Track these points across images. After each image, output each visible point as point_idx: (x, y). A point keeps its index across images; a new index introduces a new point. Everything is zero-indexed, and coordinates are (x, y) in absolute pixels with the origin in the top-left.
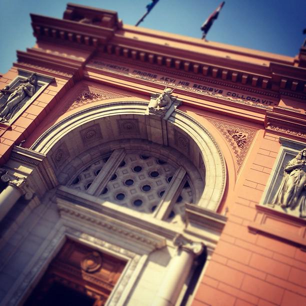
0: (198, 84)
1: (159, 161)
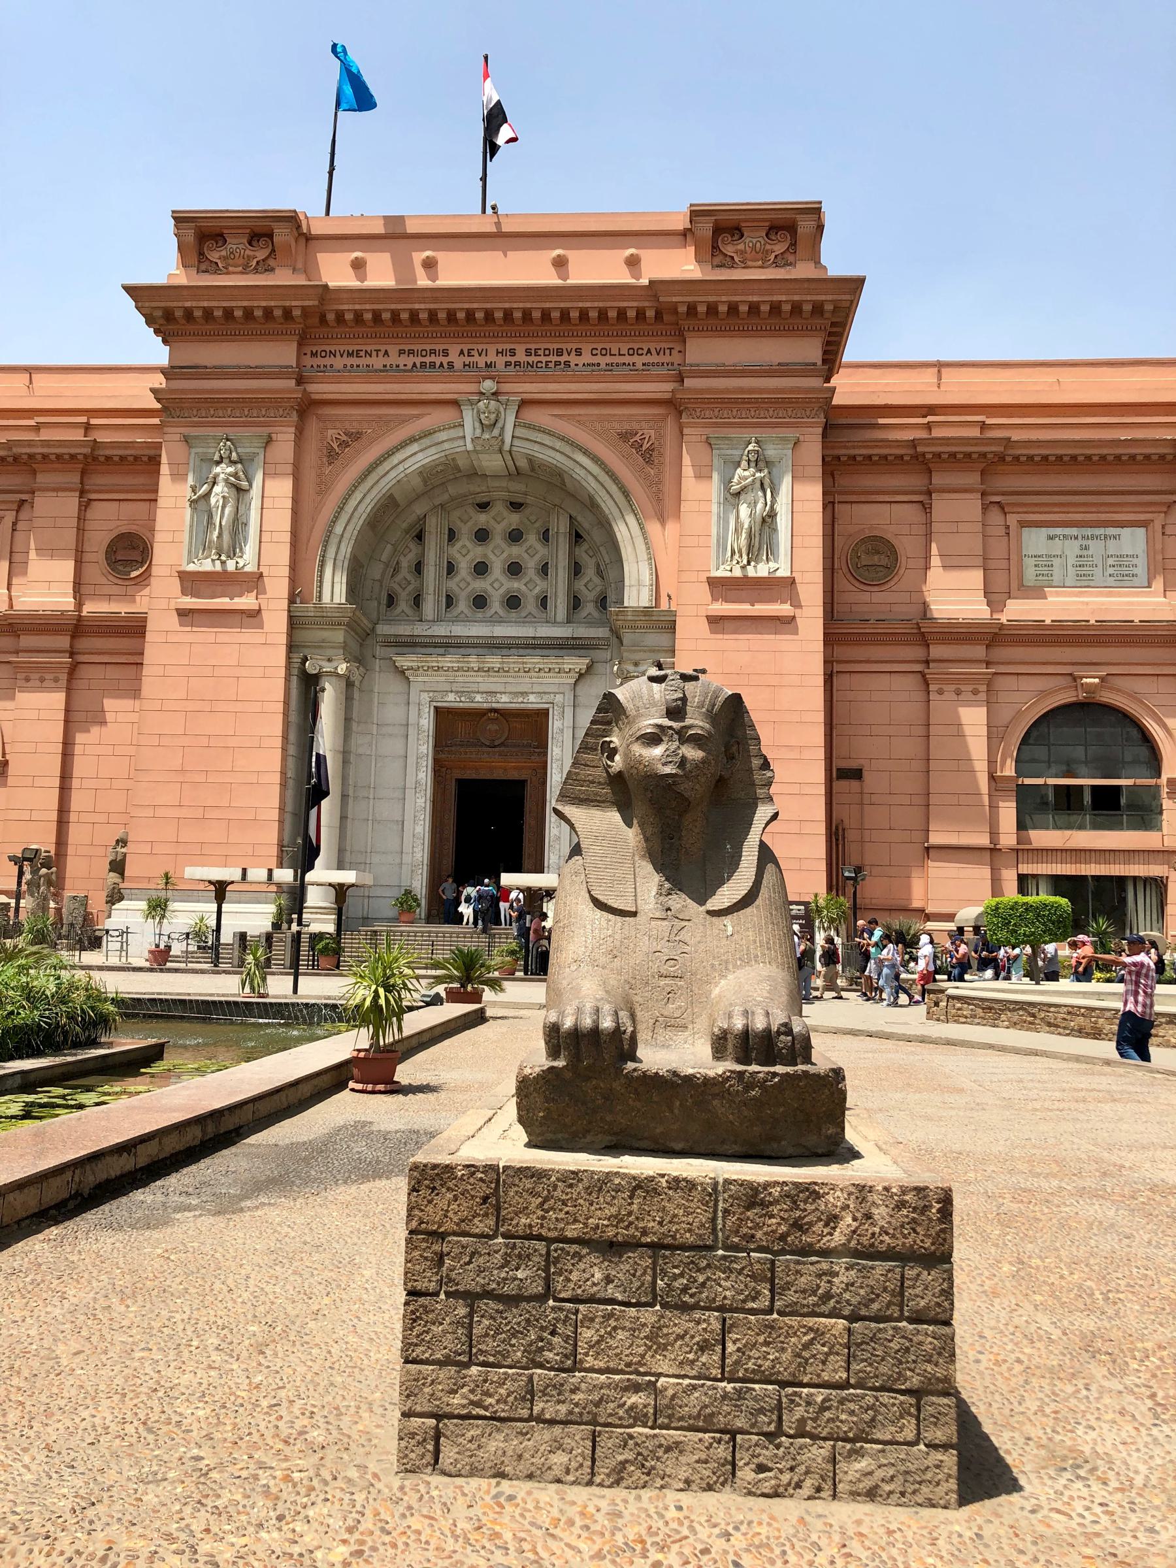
0: (533, 346)
1: (511, 503)
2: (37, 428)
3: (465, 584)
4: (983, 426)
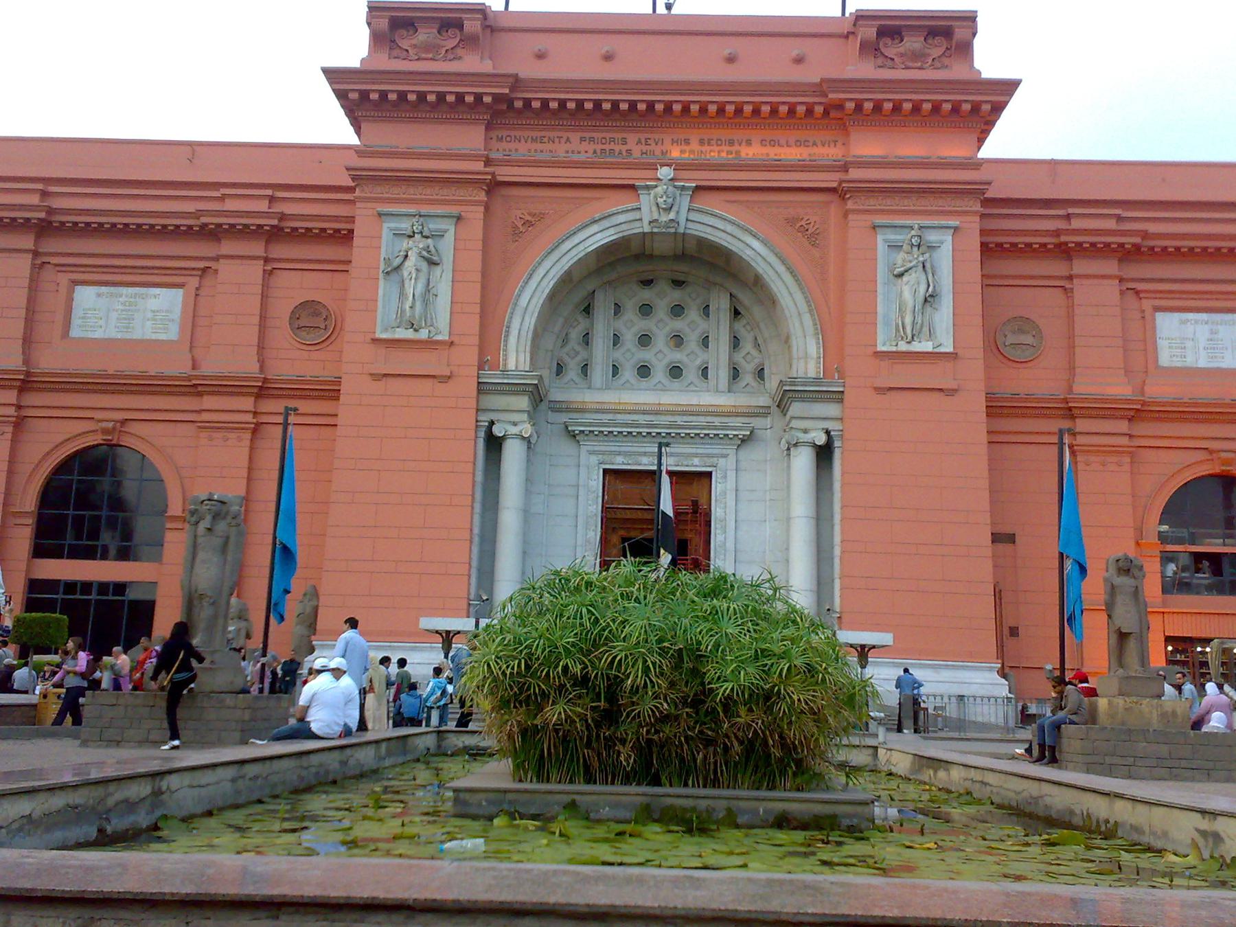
1: (673, 281)
2: (222, 198)
3: (630, 355)
4: (1119, 218)
